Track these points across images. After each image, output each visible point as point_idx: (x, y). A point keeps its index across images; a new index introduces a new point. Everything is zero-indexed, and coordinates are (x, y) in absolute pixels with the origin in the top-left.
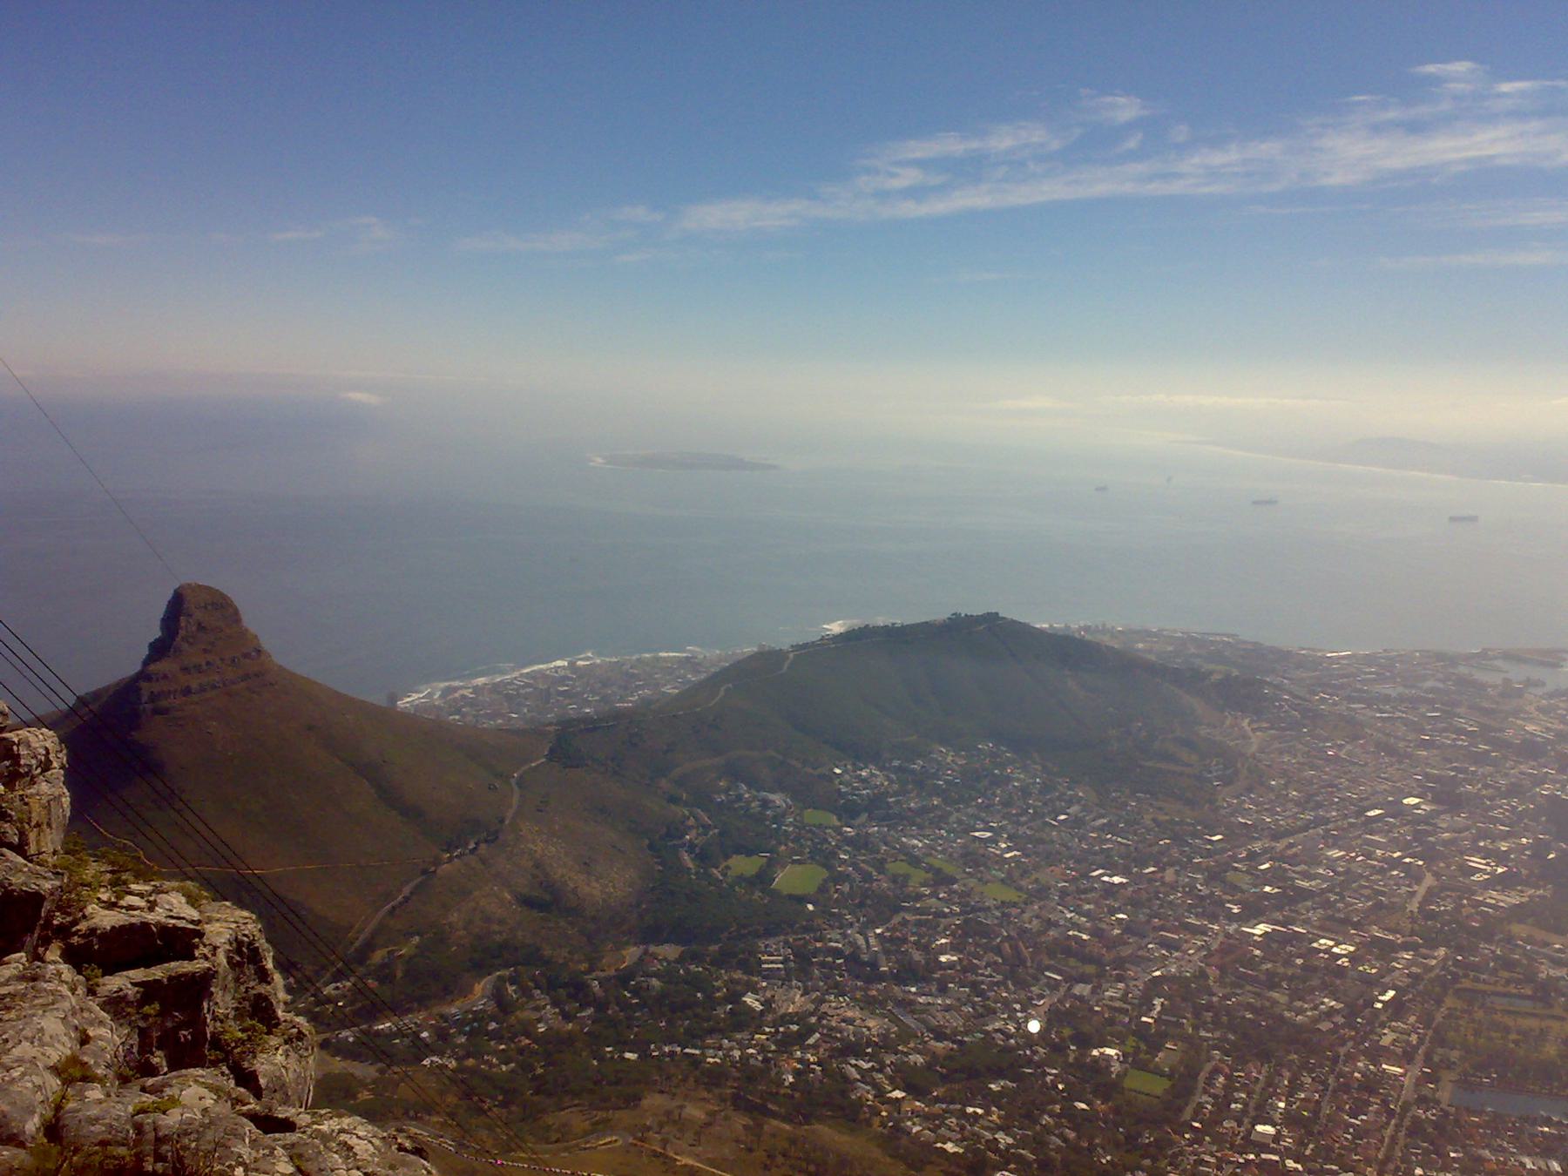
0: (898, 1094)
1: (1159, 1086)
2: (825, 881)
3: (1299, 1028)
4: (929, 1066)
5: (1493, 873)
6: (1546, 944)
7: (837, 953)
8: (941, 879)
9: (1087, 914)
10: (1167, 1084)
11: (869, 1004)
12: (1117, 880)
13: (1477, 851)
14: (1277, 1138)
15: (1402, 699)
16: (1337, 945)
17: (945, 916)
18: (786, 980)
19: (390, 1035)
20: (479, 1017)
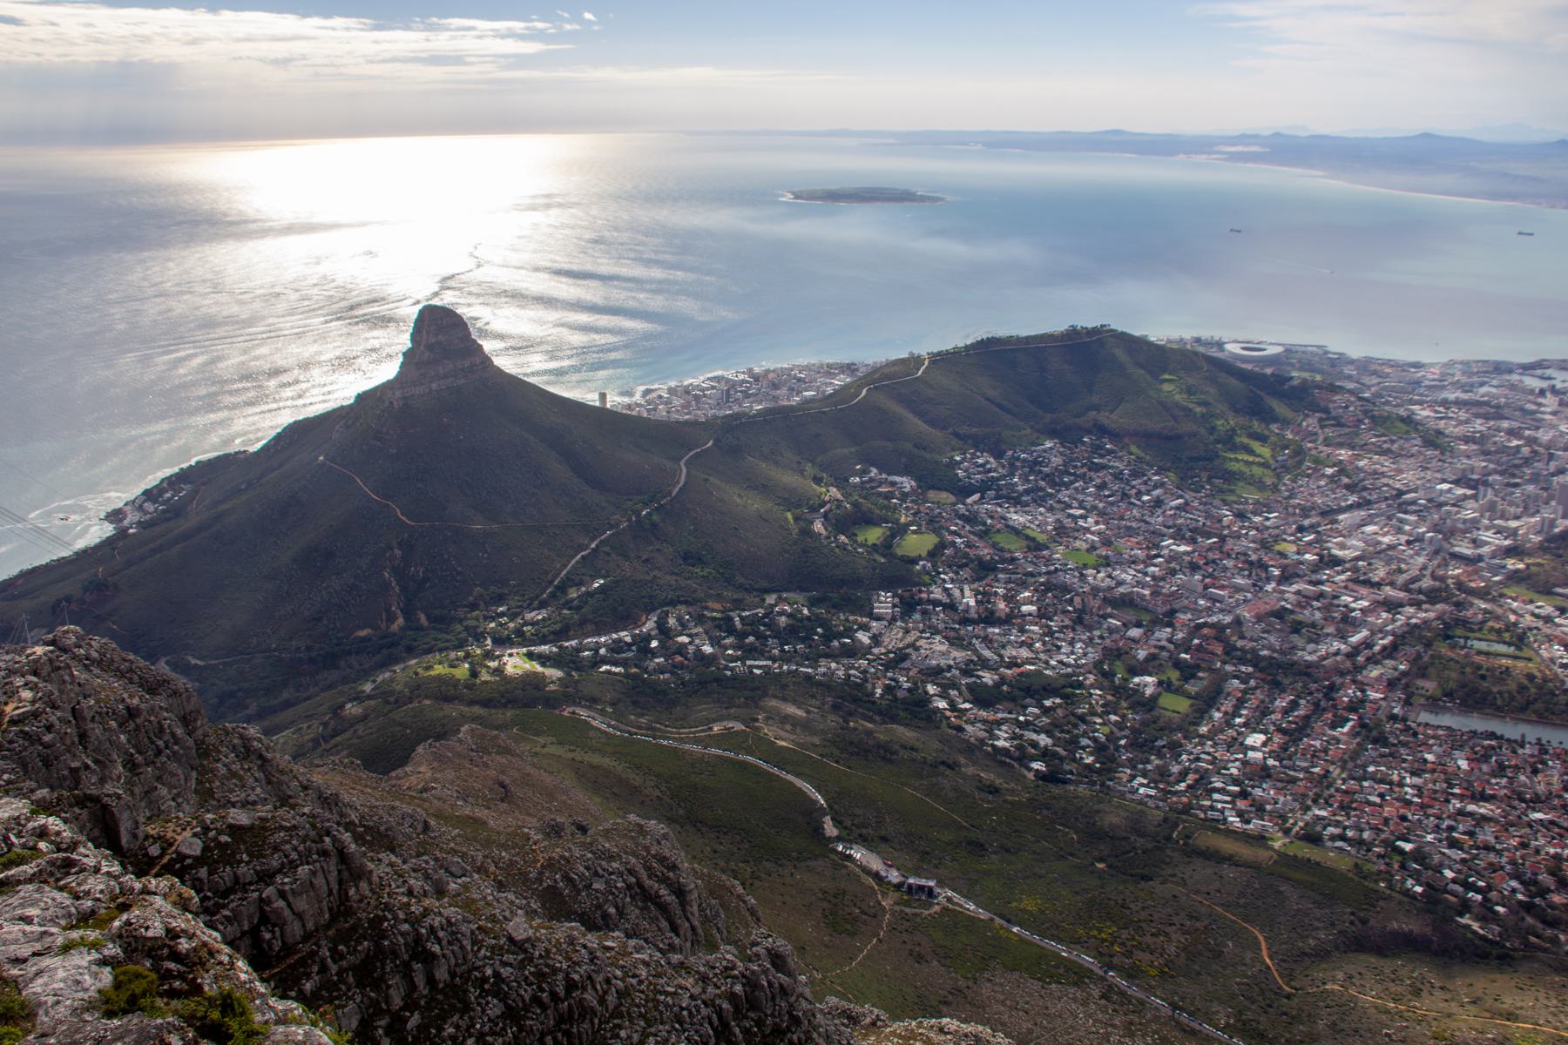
0: (967, 705)
1: (1182, 705)
2: (936, 547)
3: (1309, 665)
4: (997, 685)
5: (1499, 548)
6: (1531, 602)
7: (936, 603)
8: (1035, 547)
9: (1154, 578)
10: (1190, 702)
11: (956, 641)
12: (1183, 548)
13: (1487, 529)
14: (1264, 744)
15: (1457, 403)
16: (1357, 599)
17: (1031, 574)
18: (893, 620)
19: (578, 650)
20: (648, 638)
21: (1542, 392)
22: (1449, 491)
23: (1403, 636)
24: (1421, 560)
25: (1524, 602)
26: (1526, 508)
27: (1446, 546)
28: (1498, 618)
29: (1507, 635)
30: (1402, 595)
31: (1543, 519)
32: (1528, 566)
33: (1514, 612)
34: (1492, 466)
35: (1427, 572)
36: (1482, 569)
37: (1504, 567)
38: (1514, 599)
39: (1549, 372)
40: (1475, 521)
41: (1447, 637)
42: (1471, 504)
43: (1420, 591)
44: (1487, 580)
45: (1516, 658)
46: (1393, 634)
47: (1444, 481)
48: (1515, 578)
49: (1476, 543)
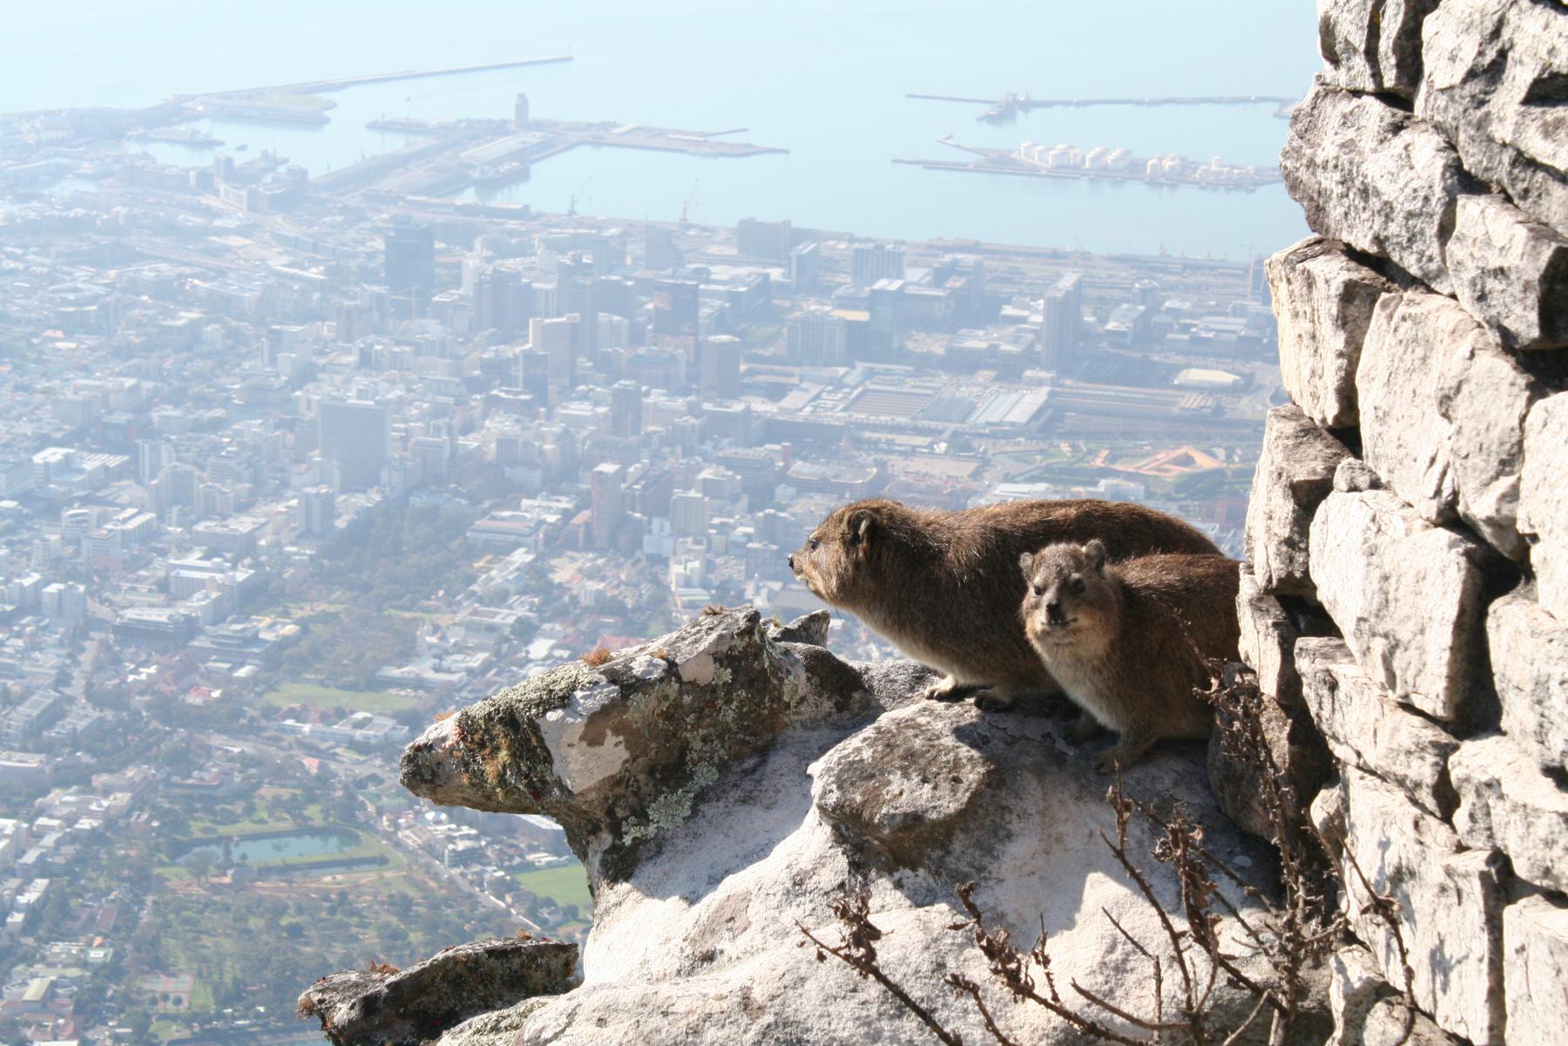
6: (341, 714)
13: (184, 548)
21: (205, 181)
22: (67, 465)
23: (70, 870)
24: (48, 661)
25: (325, 718)
26: (256, 480)
27: (104, 612)
28: (280, 774)
29: (313, 811)
30: (33, 762)
31: (307, 501)
32: (304, 624)
33: (312, 750)
34: (148, 385)
35: (77, 687)
36: (204, 655)
37: (254, 640)
38: (300, 716)
39: (204, 127)
40: (147, 535)
41: (178, 850)
42: (127, 490)
43: (75, 741)
44: (226, 680)
45: (350, 864)
46: (43, 868)
47: (44, 442)
48: (281, 661)
49: (169, 589)
